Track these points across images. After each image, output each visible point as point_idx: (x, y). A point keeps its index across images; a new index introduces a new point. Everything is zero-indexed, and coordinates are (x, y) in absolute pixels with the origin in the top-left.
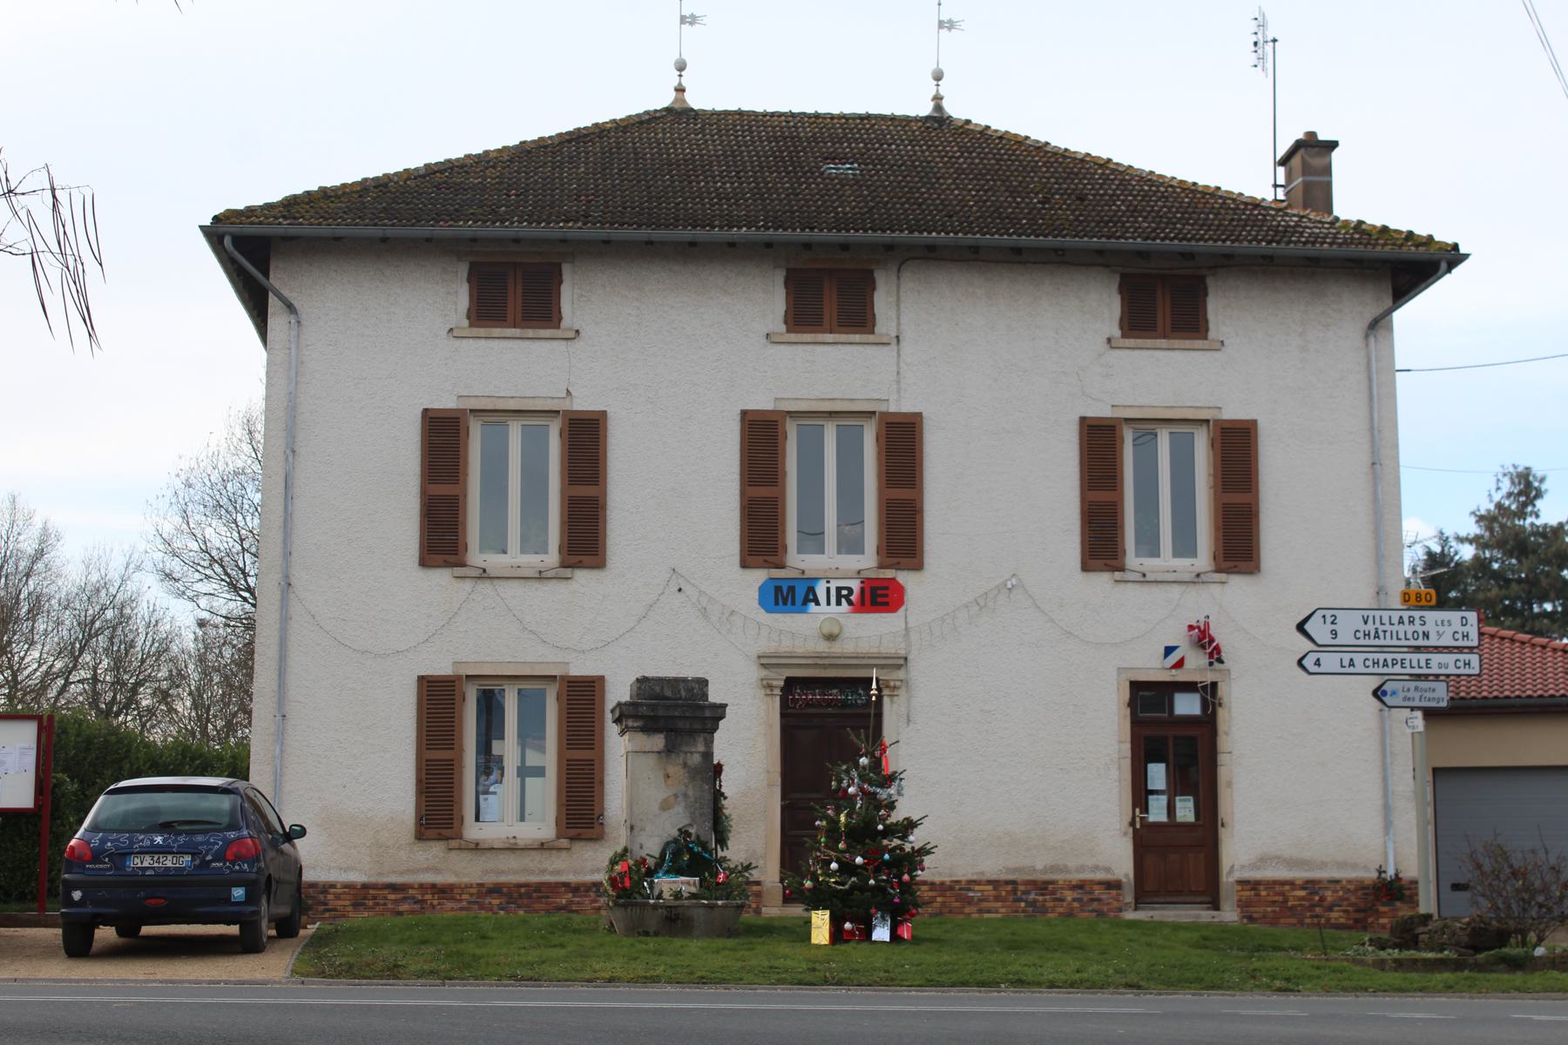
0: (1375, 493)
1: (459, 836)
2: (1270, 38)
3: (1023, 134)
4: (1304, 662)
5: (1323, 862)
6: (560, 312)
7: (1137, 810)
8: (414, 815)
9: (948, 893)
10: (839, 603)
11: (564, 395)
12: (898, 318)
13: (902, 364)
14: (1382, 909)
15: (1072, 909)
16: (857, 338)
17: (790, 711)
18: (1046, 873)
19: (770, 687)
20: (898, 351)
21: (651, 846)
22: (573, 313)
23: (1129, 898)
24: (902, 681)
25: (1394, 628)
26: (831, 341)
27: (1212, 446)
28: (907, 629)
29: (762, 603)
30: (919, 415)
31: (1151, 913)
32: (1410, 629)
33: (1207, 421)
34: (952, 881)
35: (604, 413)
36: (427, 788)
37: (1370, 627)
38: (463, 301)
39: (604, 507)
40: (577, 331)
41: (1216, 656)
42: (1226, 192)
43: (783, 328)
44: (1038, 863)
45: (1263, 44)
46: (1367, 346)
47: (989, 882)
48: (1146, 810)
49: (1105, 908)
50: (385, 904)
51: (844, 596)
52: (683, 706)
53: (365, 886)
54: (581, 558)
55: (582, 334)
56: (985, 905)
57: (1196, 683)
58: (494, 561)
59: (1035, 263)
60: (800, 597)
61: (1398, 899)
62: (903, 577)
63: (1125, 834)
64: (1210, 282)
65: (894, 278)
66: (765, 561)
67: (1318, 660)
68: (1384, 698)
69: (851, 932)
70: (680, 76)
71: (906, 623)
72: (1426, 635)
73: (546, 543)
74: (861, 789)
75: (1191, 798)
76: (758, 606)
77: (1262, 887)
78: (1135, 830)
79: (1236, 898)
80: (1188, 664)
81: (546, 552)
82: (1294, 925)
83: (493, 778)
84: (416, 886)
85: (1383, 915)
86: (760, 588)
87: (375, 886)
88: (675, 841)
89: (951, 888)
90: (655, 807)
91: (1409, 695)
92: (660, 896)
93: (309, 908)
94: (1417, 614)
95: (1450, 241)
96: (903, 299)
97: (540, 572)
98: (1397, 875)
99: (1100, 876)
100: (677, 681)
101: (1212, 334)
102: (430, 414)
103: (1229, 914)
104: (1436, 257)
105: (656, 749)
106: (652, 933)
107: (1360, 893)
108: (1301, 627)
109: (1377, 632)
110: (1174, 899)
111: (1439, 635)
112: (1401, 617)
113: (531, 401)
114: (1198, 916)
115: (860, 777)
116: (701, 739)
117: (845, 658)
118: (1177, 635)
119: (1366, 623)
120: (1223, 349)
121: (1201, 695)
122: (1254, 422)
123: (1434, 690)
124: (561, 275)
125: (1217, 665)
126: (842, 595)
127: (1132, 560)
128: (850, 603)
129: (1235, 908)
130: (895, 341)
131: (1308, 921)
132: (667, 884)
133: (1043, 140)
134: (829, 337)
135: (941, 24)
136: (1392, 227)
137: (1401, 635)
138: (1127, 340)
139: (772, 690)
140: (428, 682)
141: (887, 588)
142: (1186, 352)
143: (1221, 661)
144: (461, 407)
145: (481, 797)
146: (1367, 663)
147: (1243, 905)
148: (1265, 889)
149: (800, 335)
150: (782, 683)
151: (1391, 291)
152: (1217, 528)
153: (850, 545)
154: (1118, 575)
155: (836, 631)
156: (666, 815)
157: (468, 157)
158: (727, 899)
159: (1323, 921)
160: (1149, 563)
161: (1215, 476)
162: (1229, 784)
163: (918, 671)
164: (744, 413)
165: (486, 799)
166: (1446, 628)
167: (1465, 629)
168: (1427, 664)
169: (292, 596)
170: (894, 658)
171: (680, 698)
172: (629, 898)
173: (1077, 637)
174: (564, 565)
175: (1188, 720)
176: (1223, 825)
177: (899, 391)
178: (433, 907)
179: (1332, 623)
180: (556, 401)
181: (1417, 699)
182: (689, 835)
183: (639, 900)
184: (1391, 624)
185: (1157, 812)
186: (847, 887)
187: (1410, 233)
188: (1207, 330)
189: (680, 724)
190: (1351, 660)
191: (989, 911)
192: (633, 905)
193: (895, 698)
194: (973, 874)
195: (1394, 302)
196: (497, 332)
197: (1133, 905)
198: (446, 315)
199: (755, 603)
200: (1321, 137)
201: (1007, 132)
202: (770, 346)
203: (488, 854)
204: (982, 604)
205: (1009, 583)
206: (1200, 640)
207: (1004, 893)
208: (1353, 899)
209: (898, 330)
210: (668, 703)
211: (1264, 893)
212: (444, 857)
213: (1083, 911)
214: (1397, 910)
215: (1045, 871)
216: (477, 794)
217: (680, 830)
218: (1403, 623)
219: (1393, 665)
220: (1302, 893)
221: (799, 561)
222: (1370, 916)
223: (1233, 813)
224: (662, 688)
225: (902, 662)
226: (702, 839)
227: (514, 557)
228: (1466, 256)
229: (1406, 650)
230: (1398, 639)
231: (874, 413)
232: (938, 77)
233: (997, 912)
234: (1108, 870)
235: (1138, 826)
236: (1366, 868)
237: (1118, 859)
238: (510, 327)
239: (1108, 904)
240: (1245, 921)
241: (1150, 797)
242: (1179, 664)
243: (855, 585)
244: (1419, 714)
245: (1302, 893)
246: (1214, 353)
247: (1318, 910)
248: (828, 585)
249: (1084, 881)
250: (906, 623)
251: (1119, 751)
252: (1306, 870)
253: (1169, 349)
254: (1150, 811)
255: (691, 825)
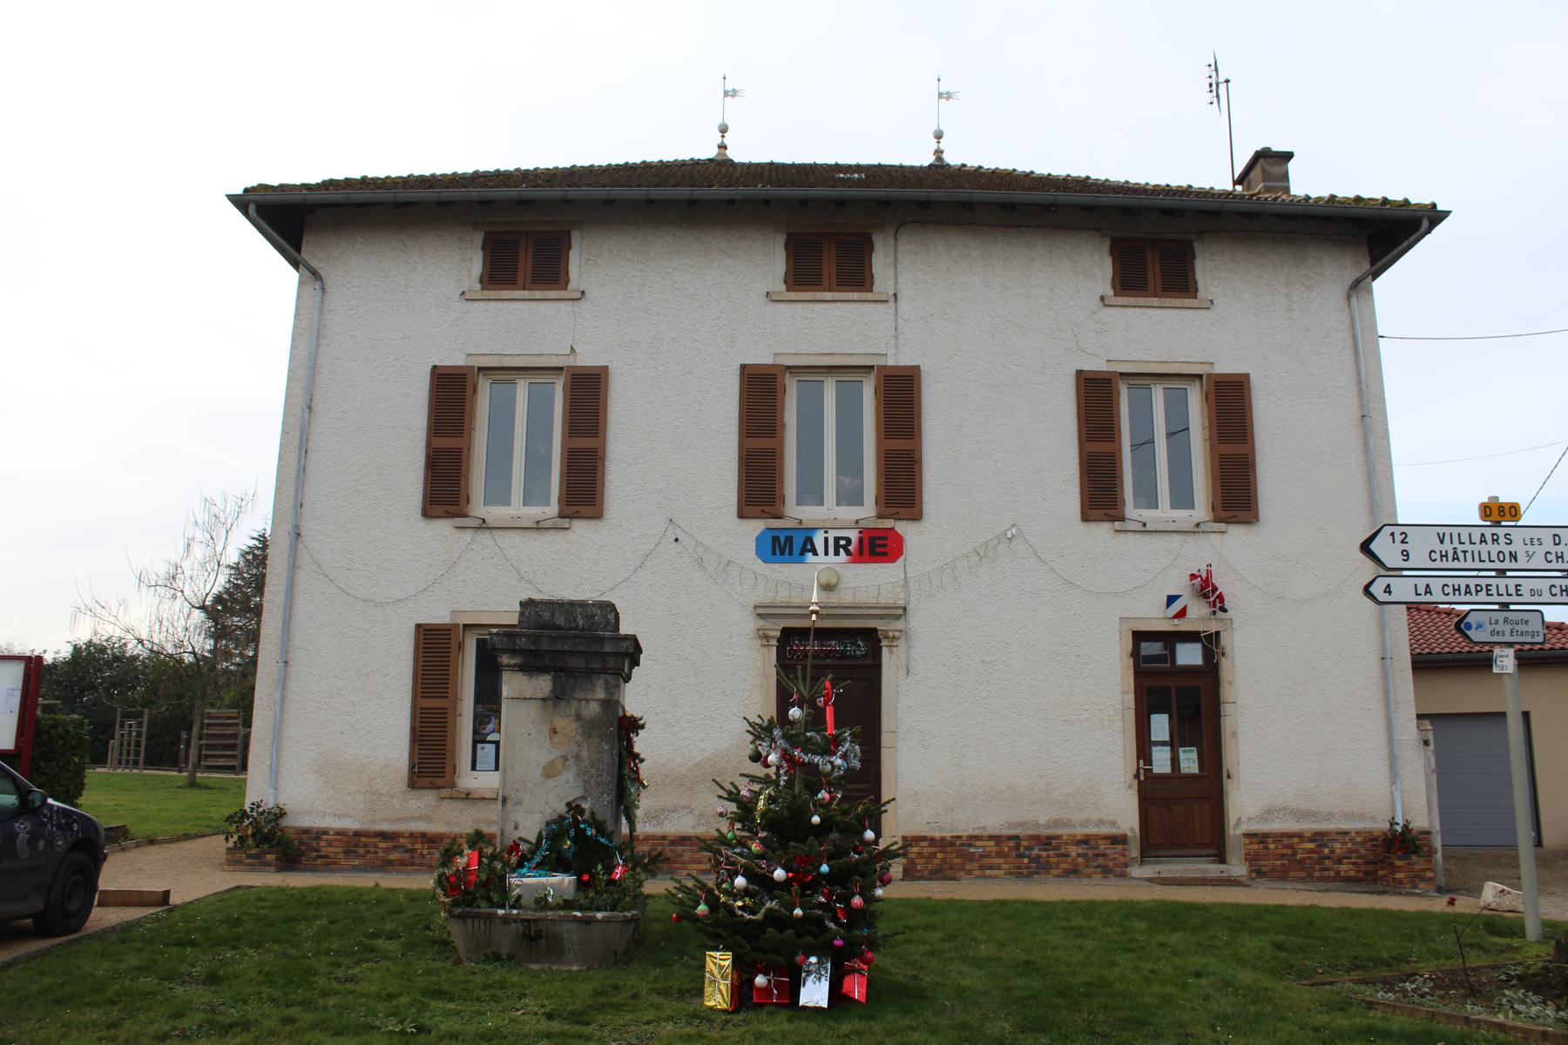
0: (1366, 446)
1: (453, 785)
2: (1221, 79)
3: (1010, 168)
4: (1372, 589)
5: (1330, 814)
6: (567, 275)
7: (1141, 762)
8: (407, 763)
9: (948, 849)
10: (837, 553)
11: (568, 351)
12: (896, 278)
13: (900, 321)
14: (1398, 863)
15: (1077, 865)
16: (855, 296)
17: (787, 662)
18: (1049, 827)
19: (766, 637)
20: (896, 307)
21: (529, 825)
22: (580, 276)
23: (1135, 852)
24: (901, 631)
25: (1476, 548)
26: (830, 299)
27: (1207, 399)
28: (906, 578)
29: (759, 553)
30: (917, 368)
31: (1158, 868)
32: (1494, 549)
33: (1200, 376)
34: (952, 837)
35: (605, 368)
36: (421, 736)
37: (1447, 547)
38: (476, 264)
39: (603, 458)
40: (583, 293)
41: (1218, 605)
42: (1199, 188)
43: (783, 287)
44: (1038, 817)
45: (1217, 86)
46: (1349, 306)
47: (991, 838)
48: (1149, 761)
49: (1111, 864)
50: (375, 852)
51: (843, 546)
52: (576, 637)
53: (357, 834)
54: (579, 508)
55: (588, 295)
56: (986, 861)
57: (1199, 633)
58: (495, 513)
59: (1028, 227)
60: (797, 546)
61: (1414, 853)
62: (902, 527)
63: (1130, 787)
64: (1197, 246)
65: (891, 240)
66: (763, 511)
67: (1388, 586)
68: (1467, 632)
69: (766, 991)
70: (723, 136)
71: (905, 572)
72: (1513, 556)
73: (549, 496)
74: (786, 756)
75: (1194, 748)
76: (765, 565)
77: (1270, 840)
78: (1140, 783)
79: (1243, 851)
80: (1190, 614)
81: (547, 503)
82: (1304, 878)
83: (490, 727)
84: (407, 835)
85: (1399, 869)
86: (757, 538)
87: (366, 834)
88: (562, 818)
89: (952, 844)
90: (537, 774)
91: (1498, 628)
92: (517, 903)
93: (303, 854)
94: (1500, 532)
95: (1427, 202)
96: (900, 258)
97: (538, 522)
98: (1406, 827)
99: (1105, 830)
100: (573, 604)
101: (1201, 294)
102: (438, 371)
103: (1237, 867)
104: (1419, 214)
105: (540, 695)
106: (505, 956)
107: (1369, 844)
108: (1365, 547)
109: (1455, 553)
110: (1179, 852)
111: (1529, 556)
112: (1483, 535)
113: (536, 358)
114: (1207, 871)
115: (785, 737)
116: (602, 682)
117: (843, 607)
118: (1178, 583)
119: (1442, 542)
120: (1212, 307)
121: (1204, 645)
122: (1247, 376)
123: (1527, 622)
124: (570, 241)
125: (1220, 614)
126: (840, 545)
127: (1130, 510)
128: (848, 553)
129: (1243, 862)
130: (893, 298)
131: (1317, 874)
132: (526, 882)
133: (1028, 170)
134: (828, 295)
135: (940, 95)
136: (1365, 195)
137: (1485, 557)
138: (1120, 298)
139: (768, 641)
140: (425, 630)
141: (886, 539)
142: (1177, 311)
143: (1224, 610)
144: (469, 364)
145: (479, 746)
146: (1447, 590)
147: (1251, 858)
148: (1274, 842)
149: (799, 293)
150: (778, 634)
151: (1368, 256)
152: (1214, 479)
153: (849, 496)
154: (1118, 525)
155: (833, 580)
156: (551, 782)
157: (518, 170)
158: (613, 908)
159: (1332, 874)
160: (1147, 514)
161: (1210, 428)
162: (1234, 735)
163: (917, 622)
164: (743, 367)
165: (483, 748)
166: (1536, 548)
167: (1559, 549)
168: (1517, 590)
169: (301, 546)
170: (892, 608)
171: (576, 628)
172: (470, 905)
173: (1079, 586)
174: (562, 516)
175: (1190, 671)
176: (1229, 777)
177: (897, 346)
178: (423, 856)
179: (1402, 542)
180: (561, 357)
181: (1508, 632)
182: (582, 812)
183: (484, 909)
184: (1471, 543)
185: (1161, 761)
186: (759, 917)
187: (1385, 201)
188: (1196, 291)
189: (572, 662)
190: (1428, 586)
191: (991, 868)
192: (473, 917)
193: (894, 649)
194: (974, 830)
195: (1372, 265)
196: (506, 294)
197: (1139, 859)
198: (460, 280)
199: (753, 554)
200: (1274, 149)
201: (997, 168)
202: (770, 304)
203: (480, 804)
204: (982, 554)
205: (1009, 532)
206: (1203, 588)
207: (1006, 849)
208: (1362, 851)
209: (896, 288)
210: (555, 633)
211: (1272, 846)
212: (436, 806)
213: (1088, 866)
214: (1414, 864)
215: (1048, 825)
216: (475, 743)
217: (568, 804)
218: (1485, 541)
219: (1477, 591)
220: (1311, 846)
221: (797, 512)
222: (1381, 869)
223: (1239, 764)
224: (553, 614)
225: (900, 612)
226: (599, 817)
227: (516, 509)
228: (1446, 214)
229: (1493, 574)
230: (1481, 561)
231: (872, 367)
232: (939, 136)
233: (1000, 869)
234: (1113, 824)
235: (1142, 778)
236: (1373, 819)
237: (1123, 812)
238: (519, 289)
239: (1114, 859)
240: (1254, 875)
241: (1154, 749)
242: (1182, 614)
243: (854, 535)
244: (1510, 652)
245: (1311, 846)
246: (1204, 312)
247: (1326, 862)
248: (826, 535)
249: (1089, 836)
250: (905, 572)
251: (1123, 702)
252: (1314, 822)
253: (1160, 307)
254: (1154, 764)
255: (584, 798)
